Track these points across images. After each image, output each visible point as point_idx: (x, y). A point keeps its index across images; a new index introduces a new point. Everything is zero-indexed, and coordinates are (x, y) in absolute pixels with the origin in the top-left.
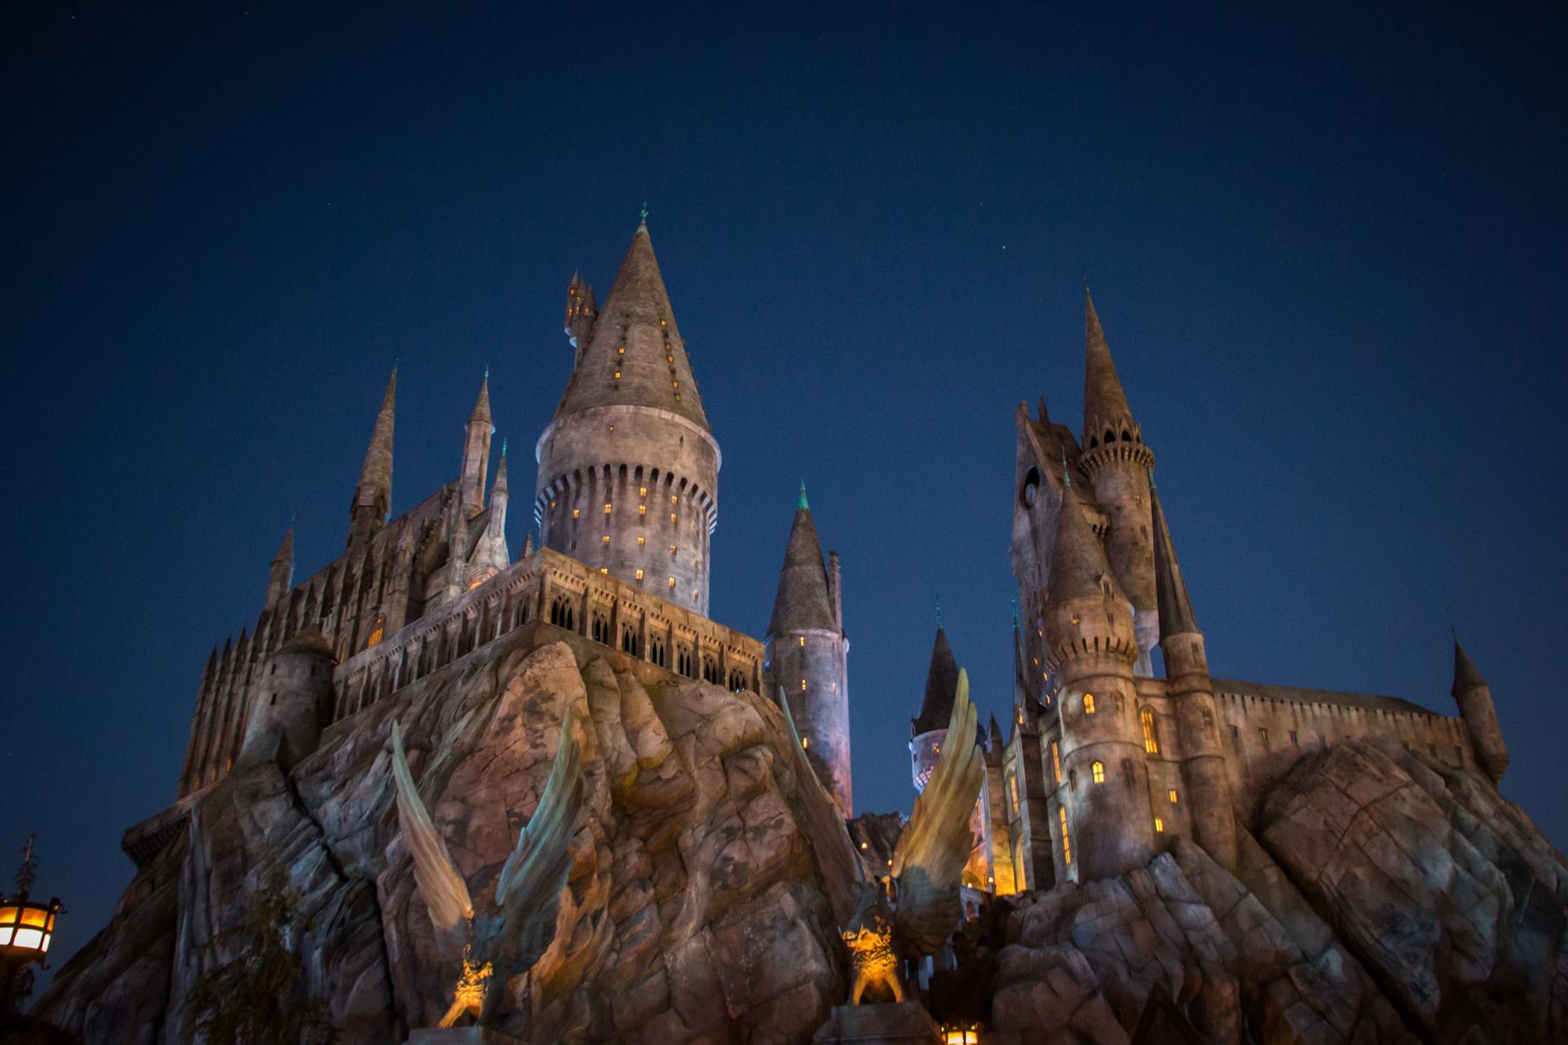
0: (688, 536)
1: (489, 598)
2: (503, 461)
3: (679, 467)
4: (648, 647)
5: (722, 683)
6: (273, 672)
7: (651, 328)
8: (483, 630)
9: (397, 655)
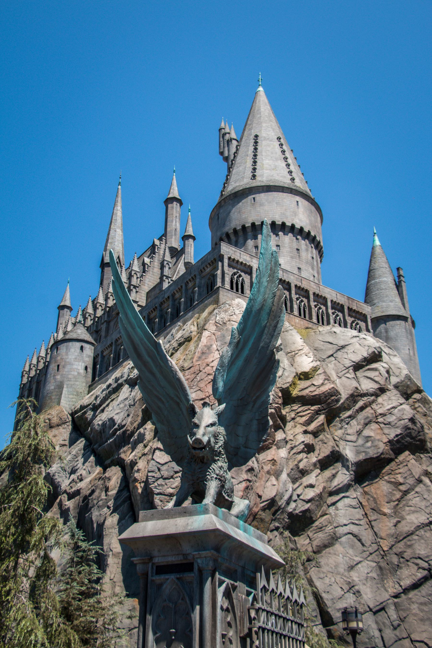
1: (188, 283)
4: (295, 307)
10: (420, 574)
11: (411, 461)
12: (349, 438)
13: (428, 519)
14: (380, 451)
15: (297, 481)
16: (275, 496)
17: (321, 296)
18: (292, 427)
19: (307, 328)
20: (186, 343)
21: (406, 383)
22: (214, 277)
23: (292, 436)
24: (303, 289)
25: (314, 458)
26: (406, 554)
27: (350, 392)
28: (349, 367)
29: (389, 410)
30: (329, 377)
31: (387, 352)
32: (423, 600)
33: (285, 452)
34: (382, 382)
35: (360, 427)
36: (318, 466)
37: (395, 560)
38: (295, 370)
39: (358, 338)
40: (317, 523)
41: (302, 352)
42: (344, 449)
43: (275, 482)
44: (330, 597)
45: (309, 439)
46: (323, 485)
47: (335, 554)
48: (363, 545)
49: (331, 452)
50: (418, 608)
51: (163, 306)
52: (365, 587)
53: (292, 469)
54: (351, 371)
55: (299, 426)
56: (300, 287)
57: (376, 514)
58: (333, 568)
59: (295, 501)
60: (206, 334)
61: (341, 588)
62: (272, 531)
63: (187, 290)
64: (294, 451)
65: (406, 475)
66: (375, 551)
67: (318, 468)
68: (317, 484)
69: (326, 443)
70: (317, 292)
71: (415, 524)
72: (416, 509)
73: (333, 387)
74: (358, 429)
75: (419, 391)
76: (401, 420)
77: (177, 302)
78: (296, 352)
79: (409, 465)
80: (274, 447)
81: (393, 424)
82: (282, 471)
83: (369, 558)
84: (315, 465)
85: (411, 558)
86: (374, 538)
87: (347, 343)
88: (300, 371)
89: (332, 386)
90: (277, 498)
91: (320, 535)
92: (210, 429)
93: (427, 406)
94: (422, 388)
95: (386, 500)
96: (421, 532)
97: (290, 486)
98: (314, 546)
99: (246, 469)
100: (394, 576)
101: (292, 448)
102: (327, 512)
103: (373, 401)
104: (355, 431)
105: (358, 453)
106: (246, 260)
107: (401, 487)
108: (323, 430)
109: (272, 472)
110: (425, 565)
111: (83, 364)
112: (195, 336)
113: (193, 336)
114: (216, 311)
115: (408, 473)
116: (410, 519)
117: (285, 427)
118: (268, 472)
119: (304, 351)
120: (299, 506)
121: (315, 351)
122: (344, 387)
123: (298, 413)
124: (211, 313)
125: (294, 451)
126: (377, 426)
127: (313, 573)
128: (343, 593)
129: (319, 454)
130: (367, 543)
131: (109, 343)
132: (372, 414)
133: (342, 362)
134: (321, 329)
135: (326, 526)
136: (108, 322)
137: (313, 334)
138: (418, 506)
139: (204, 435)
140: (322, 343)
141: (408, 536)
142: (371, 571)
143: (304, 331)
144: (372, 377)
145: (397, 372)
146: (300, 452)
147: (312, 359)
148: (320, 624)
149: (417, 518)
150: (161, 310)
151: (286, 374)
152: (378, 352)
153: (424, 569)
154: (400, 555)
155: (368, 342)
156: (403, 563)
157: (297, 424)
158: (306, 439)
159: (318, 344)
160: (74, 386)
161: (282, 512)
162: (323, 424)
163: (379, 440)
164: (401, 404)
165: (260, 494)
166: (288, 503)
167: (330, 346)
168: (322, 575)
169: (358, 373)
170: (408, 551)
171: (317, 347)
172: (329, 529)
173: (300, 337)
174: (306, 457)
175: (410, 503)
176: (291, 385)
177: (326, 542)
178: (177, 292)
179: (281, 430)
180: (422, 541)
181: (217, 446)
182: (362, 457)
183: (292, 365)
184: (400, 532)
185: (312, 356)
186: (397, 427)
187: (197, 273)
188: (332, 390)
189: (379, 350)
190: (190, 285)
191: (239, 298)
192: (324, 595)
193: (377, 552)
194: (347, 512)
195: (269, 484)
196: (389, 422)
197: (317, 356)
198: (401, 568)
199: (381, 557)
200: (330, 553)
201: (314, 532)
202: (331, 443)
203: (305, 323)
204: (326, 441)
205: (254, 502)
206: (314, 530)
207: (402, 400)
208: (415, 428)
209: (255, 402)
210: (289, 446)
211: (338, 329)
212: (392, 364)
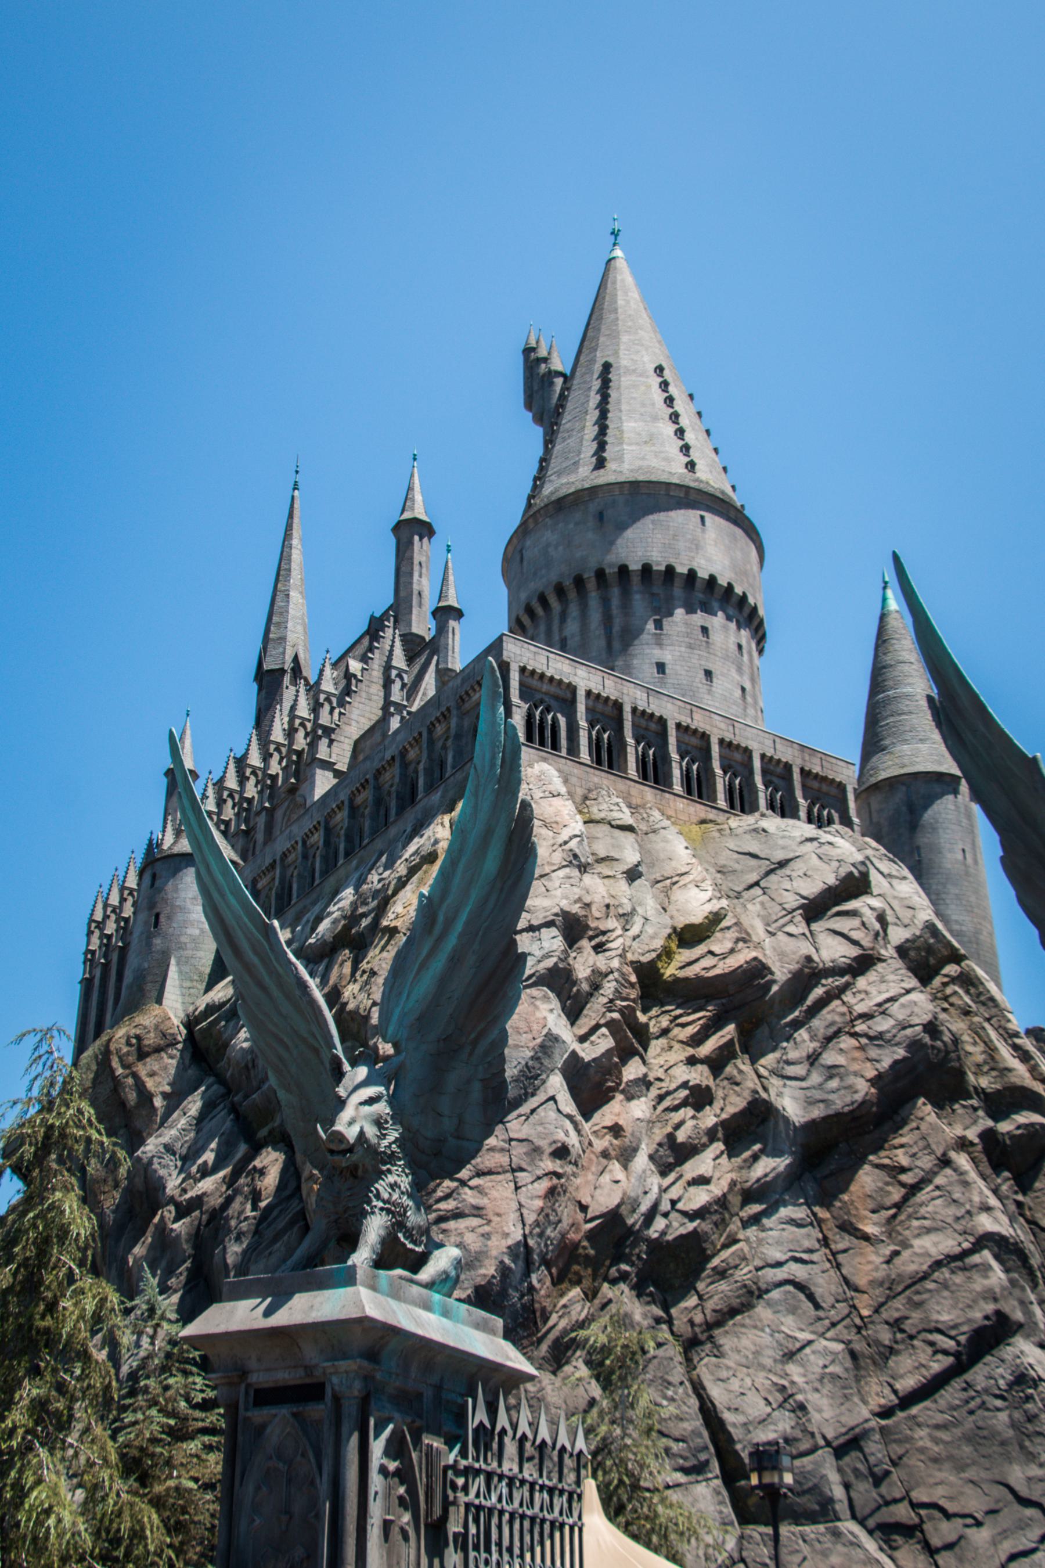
0: (726, 658)
4: (676, 773)
5: (795, 815)
6: (152, 885)
8: (428, 772)
9: (316, 836)
10: (937, 1365)
11: (928, 1118)
12: (791, 1071)
13: (960, 1244)
14: (859, 1097)
15: (671, 1171)
16: (618, 1206)
17: (738, 746)
18: (663, 1049)
19: (703, 822)
20: (425, 867)
21: (926, 941)
23: (661, 1070)
24: (695, 731)
25: (709, 1118)
26: (909, 1321)
27: (794, 967)
28: (794, 910)
29: (879, 1005)
30: (748, 934)
31: (886, 871)
32: (940, 1418)
33: (644, 1107)
34: (866, 942)
35: (815, 1045)
36: (720, 1135)
37: (885, 1336)
38: (669, 922)
39: (815, 843)
40: (715, 1262)
42: (780, 1095)
43: (620, 1174)
44: (741, 1419)
45: (700, 1075)
46: (728, 1177)
47: (755, 1327)
48: (817, 1306)
49: (749, 1103)
50: (930, 1435)
51: (381, 779)
52: (817, 1395)
53: (660, 1145)
54: (799, 918)
55: (677, 1046)
56: (687, 728)
57: (847, 1237)
59: (666, 1215)
61: (766, 1399)
62: (613, 1282)
63: (431, 742)
64: (667, 1103)
65: (915, 1149)
66: (843, 1319)
67: (718, 1140)
68: (717, 1175)
69: (737, 1084)
70: (728, 737)
71: (930, 1256)
72: (934, 1225)
73: (755, 959)
74: (811, 1050)
75: (956, 958)
76: (904, 1028)
77: (411, 768)
78: (675, 879)
79: (924, 1126)
80: (619, 1097)
81: (888, 1036)
82: (635, 1150)
83: (829, 1335)
84: (712, 1135)
85: (919, 1332)
86: (840, 1290)
87: (791, 855)
88: (681, 922)
89: (754, 954)
90: (624, 1210)
91: (723, 1286)
92: (367, 1109)
93: (972, 990)
94: (962, 951)
95: (871, 1205)
96: (944, 1274)
97: (655, 1182)
98: (708, 1312)
99: (551, 1150)
100: (881, 1370)
101: (661, 1098)
102: (741, 1236)
103: (846, 987)
104: (804, 1054)
105: (810, 1102)
106: (561, 672)
107: (904, 1178)
108: (733, 1056)
109: (613, 1153)
110: (950, 1344)
115: (921, 1144)
116: (923, 1247)
117: (646, 1050)
118: (605, 1154)
119: (691, 877)
120: (675, 1224)
121: (719, 875)
122: (782, 955)
125: (667, 1103)
126: (853, 1042)
127: (704, 1369)
128: (768, 1409)
129: (722, 1109)
130: (826, 1301)
131: (268, 861)
132: (843, 1014)
133: (778, 899)
134: (734, 822)
135: (736, 1267)
137: (716, 834)
138: (939, 1217)
139: (351, 1123)
140: (736, 856)
141: (914, 1284)
142: (833, 1362)
143: (695, 828)
144: (845, 931)
145: (905, 915)
147: (709, 894)
148: (717, 1477)
149: (935, 1244)
150: (378, 788)
151: (650, 930)
152: (860, 872)
153: (945, 1352)
154: (896, 1325)
155: (838, 851)
156: (903, 1341)
157: (674, 1043)
159: (726, 858)
160: (193, 961)
161: (634, 1245)
162: (731, 1041)
163: (856, 1074)
164: (908, 992)
165: (584, 1202)
167: (753, 862)
168: (724, 1374)
169: (814, 926)
170: (914, 1315)
171: (724, 866)
172: (743, 1274)
174: (693, 1117)
175: (923, 1211)
176: (659, 956)
177: (735, 1302)
178: (411, 745)
179: (637, 1058)
180: (946, 1293)
181: (385, 1143)
182: (817, 1112)
183: (664, 909)
184: (899, 1275)
185: (710, 888)
186: (897, 1044)
187: (452, 704)
188: (754, 963)
189: (862, 868)
190: (440, 730)
191: (545, 760)
192: (728, 1417)
193: (847, 1321)
194: (785, 1234)
195: (606, 1178)
196: (881, 1033)
197: (724, 887)
198: (897, 1353)
199: (854, 1330)
200: (743, 1326)
202: (751, 1082)
203: (699, 811)
204: (738, 1078)
205: (570, 1221)
206: (709, 1277)
207: (913, 982)
208: (939, 1043)
209: (475, 1043)
210: (654, 1092)
211: (773, 823)
212: (895, 897)
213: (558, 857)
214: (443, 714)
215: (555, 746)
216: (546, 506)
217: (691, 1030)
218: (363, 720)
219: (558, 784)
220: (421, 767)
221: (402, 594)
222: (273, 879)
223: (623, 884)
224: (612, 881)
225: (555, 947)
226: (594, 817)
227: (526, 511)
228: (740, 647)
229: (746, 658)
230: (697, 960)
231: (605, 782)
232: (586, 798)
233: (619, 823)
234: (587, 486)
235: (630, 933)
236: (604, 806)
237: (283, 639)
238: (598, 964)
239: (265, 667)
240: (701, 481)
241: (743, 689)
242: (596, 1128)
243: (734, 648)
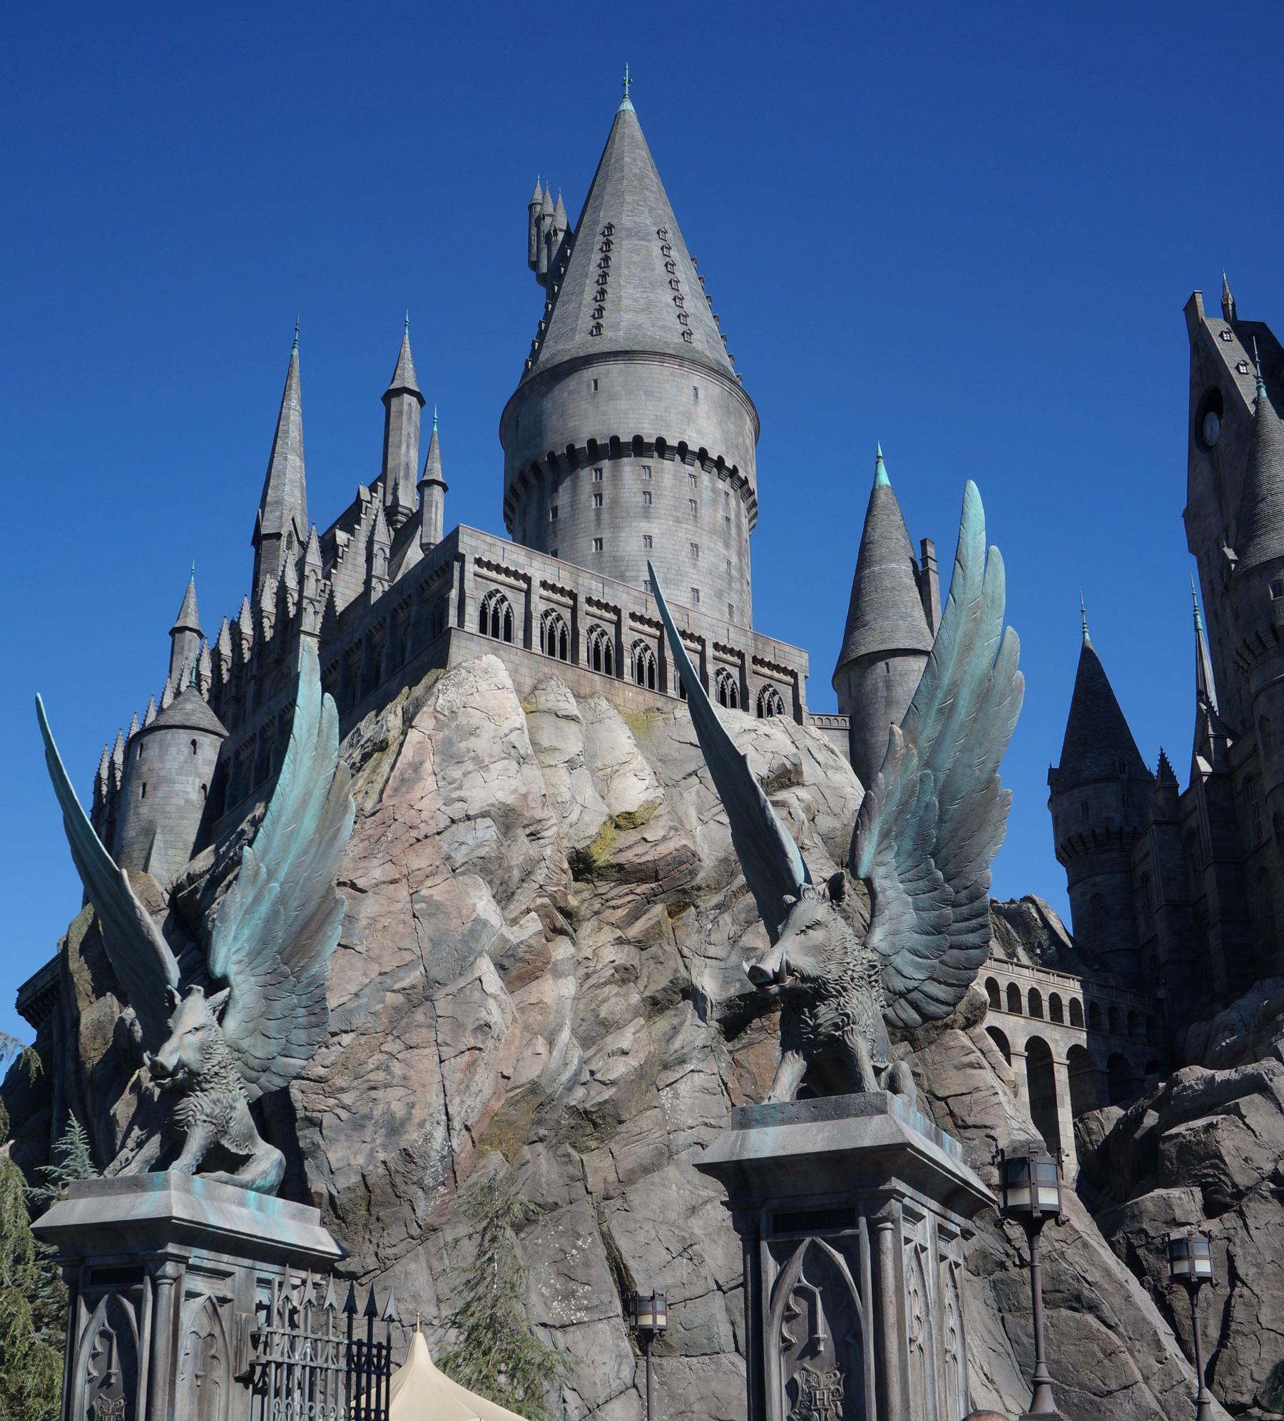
0: (714, 531)
2: (436, 438)
3: (694, 435)
4: (627, 662)
7: (644, 243)
12: (712, 951)
20: (375, 755)
22: (446, 602)
38: (606, 810)
39: (753, 735)
41: (627, 767)
42: (701, 974)
45: (622, 956)
47: (663, 1185)
55: (607, 928)
58: (657, 1211)
60: (413, 735)
61: (667, 1249)
78: (615, 768)
82: (560, 1027)
89: (684, 842)
101: (588, 976)
105: (726, 982)
106: (516, 563)
111: (197, 780)
112: (395, 740)
113: (390, 739)
114: (439, 686)
120: (593, 1093)
121: (659, 764)
123: (607, 901)
124: (429, 688)
125: (592, 981)
136: (259, 680)
137: (661, 724)
146: (605, 984)
147: (647, 782)
151: (587, 818)
158: (620, 956)
166: (569, 1089)
168: (632, 1226)
173: (629, 734)
177: (647, 1162)
178: (377, 630)
183: (602, 797)
189: (796, 761)
190: (402, 616)
200: (653, 1184)
201: (623, 1143)
213: (498, 748)
214: (404, 600)
215: (508, 637)
216: (542, 373)
217: (621, 913)
218: (348, 592)
219: (504, 677)
220: (384, 652)
221: (390, 464)
222: (254, 752)
223: (563, 772)
224: (553, 769)
225: (488, 837)
226: (540, 707)
227: (523, 377)
228: (728, 519)
229: (734, 531)
230: (629, 847)
231: (555, 671)
232: (535, 688)
233: (565, 713)
234: (582, 354)
235: (568, 821)
236: (552, 697)
237: (279, 503)
238: (531, 852)
239: (264, 531)
240: (698, 352)
241: (729, 563)
242: (522, 1005)
243: (722, 521)
